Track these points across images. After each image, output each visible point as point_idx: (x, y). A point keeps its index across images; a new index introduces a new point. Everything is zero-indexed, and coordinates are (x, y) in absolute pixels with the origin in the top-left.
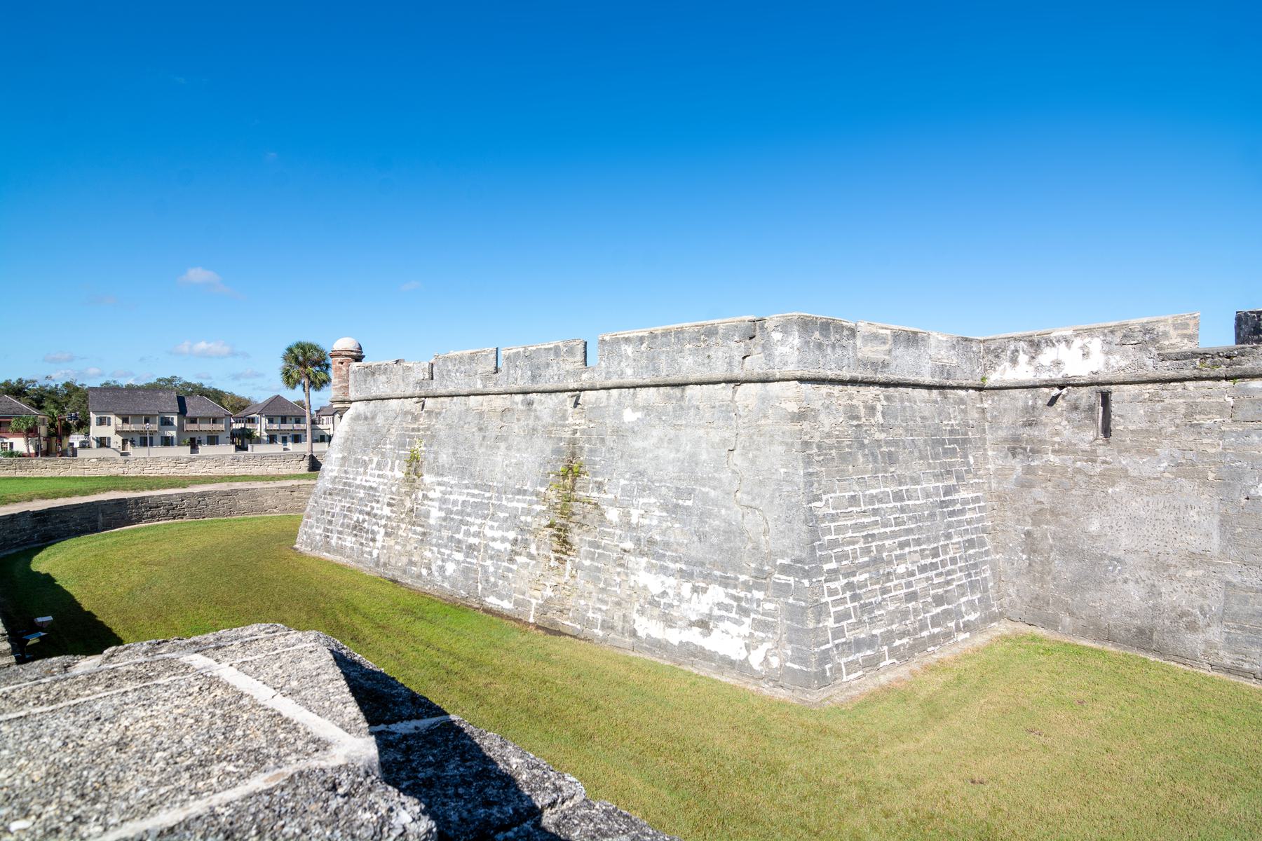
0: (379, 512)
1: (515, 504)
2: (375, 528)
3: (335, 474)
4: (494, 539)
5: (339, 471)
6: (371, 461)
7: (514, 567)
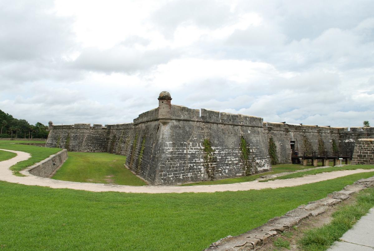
0: (199, 161)
1: (236, 152)
2: (200, 167)
3: (171, 150)
4: (234, 161)
5: (172, 149)
6: (189, 144)
7: (240, 166)
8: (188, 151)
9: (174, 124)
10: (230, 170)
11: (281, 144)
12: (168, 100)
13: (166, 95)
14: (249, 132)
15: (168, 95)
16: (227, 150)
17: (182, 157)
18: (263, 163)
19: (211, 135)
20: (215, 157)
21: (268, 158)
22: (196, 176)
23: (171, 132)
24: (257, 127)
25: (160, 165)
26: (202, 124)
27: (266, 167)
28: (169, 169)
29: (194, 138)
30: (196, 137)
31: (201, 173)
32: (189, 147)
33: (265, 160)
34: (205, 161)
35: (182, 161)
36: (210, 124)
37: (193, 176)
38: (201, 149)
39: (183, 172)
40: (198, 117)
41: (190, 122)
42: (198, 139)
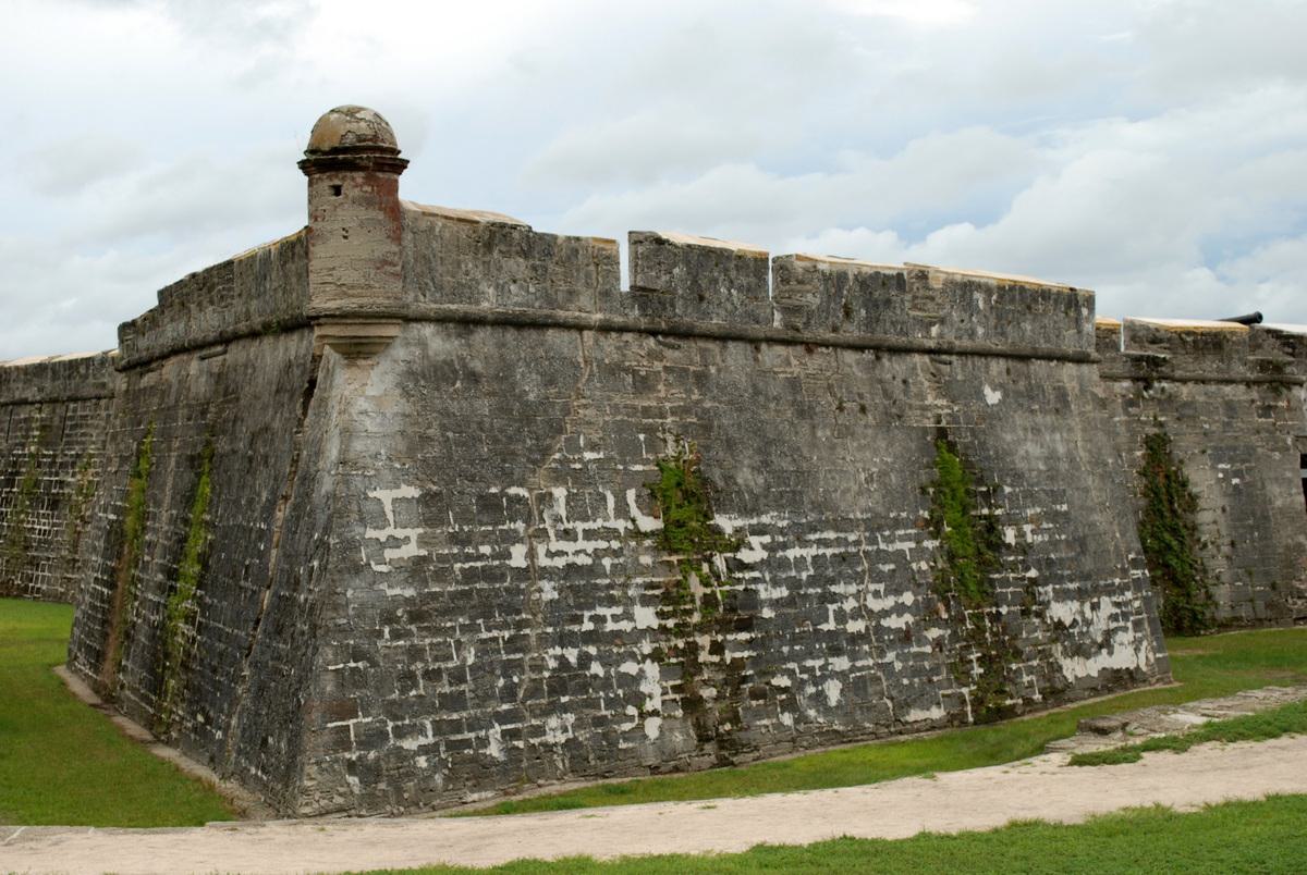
0: (625, 626)
1: (899, 545)
2: (630, 668)
3: (412, 550)
4: (886, 613)
5: (423, 541)
6: (546, 499)
7: (928, 649)
8: (541, 549)
9: (425, 356)
10: (856, 686)
11: (1235, 481)
12: (380, 175)
13: (360, 138)
14: (993, 397)
15: (375, 137)
16: (831, 535)
17: (493, 596)
18: (1101, 621)
19: (707, 428)
20: (741, 588)
21: (1137, 584)
22: (605, 736)
23: (405, 415)
24: (1049, 357)
25: (329, 661)
26: (638, 350)
27: (1123, 657)
28: (404, 691)
29: (579, 450)
30: (594, 447)
31: (642, 716)
32: (547, 525)
33: (1117, 605)
34: (670, 623)
35: (500, 627)
36: (701, 344)
37: (583, 735)
38: (637, 534)
39: (505, 707)
40: (606, 294)
41: (550, 332)
42: (611, 459)
